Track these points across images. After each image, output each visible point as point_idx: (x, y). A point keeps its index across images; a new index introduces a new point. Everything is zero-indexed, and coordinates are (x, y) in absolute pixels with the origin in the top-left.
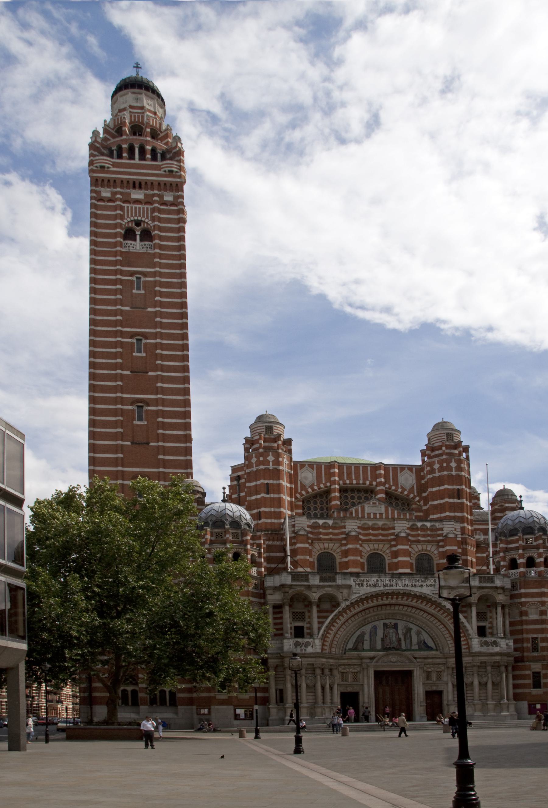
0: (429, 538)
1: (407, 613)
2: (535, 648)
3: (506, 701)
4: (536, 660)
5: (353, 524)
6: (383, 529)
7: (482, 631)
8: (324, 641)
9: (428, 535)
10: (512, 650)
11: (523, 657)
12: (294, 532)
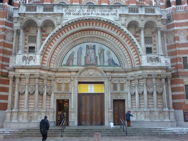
1: (100, 37)
3: (167, 109)
8: (44, 57)
11: (178, 72)
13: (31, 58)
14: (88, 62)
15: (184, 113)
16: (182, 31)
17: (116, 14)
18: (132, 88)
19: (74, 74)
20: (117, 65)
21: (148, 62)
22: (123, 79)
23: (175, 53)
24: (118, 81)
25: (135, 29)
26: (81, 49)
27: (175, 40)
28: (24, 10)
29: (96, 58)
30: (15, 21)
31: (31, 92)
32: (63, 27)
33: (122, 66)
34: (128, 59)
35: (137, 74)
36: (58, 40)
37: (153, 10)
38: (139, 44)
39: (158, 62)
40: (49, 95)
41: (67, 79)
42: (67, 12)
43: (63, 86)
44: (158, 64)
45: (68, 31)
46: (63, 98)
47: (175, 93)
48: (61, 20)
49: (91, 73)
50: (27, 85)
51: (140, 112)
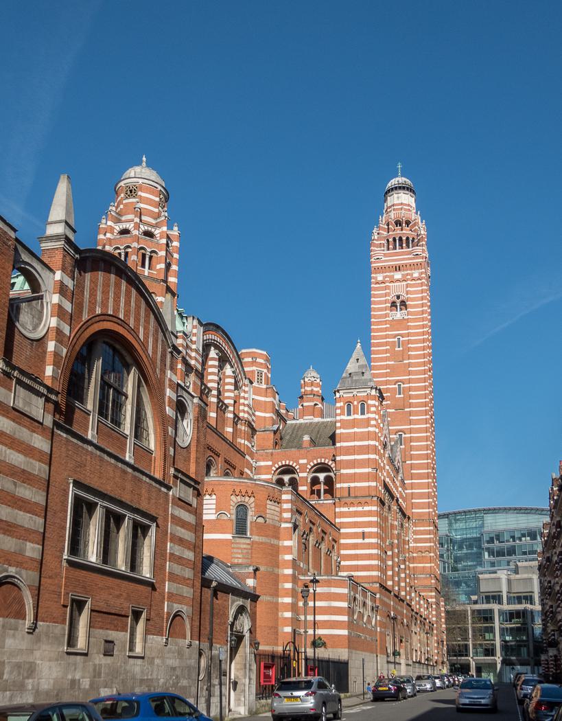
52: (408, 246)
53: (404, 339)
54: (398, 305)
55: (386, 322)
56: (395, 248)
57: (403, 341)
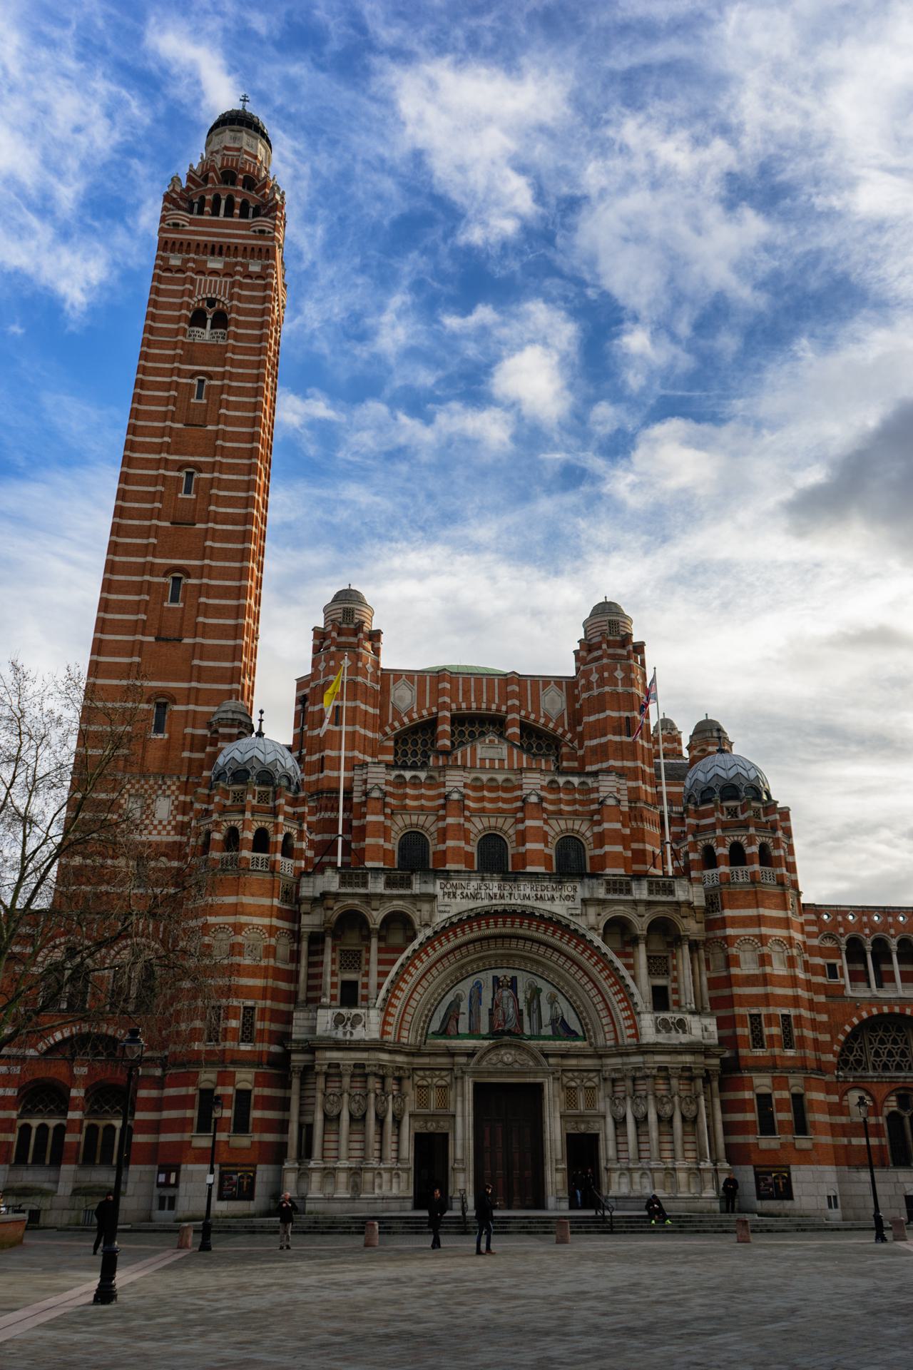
0: (577, 807)
1: (531, 955)
2: (758, 1041)
3: (707, 1164)
4: (759, 1068)
5: (458, 778)
6: (506, 790)
7: (660, 999)
9: (573, 802)
10: (716, 1041)
11: (737, 1057)
12: (366, 793)
13: (356, 1020)
14: (499, 1025)
15: (757, 1174)
16: (747, 941)
17: (573, 897)
18: (617, 1101)
19: (462, 1060)
20: (577, 1035)
21: (658, 1031)
22: (592, 1075)
23: (730, 1001)
24: (578, 1081)
25: (623, 934)
26: (478, 987)
27: (728, 966)
28: (334, 884)
29: (520, 1013)
30: (305, 907)
31: (358, 1115)
32: (436, 933)
33: (590, 1038)
34: (605, 1021)
35: (630, 1063)
36: (422, 967)
37: (670, 885)
38: (634, 978)
39: (684, 1032)
40: (398, 1122)
41: (444, 1073)
42: (446, 890)
43: (433, 1095)
44: (684, 1038)
45: (449, 940)
46: (432, 1127)
47: (733, 1115)
48: (432, 914)
49: (508, 1058)
50: (346, 1095)
51: (640, 1172)
52: (244, 214)
53: (213, 382)
54: (209, 316)
55: (175, 346)
56: (215, 213)
57: (209, 386)
